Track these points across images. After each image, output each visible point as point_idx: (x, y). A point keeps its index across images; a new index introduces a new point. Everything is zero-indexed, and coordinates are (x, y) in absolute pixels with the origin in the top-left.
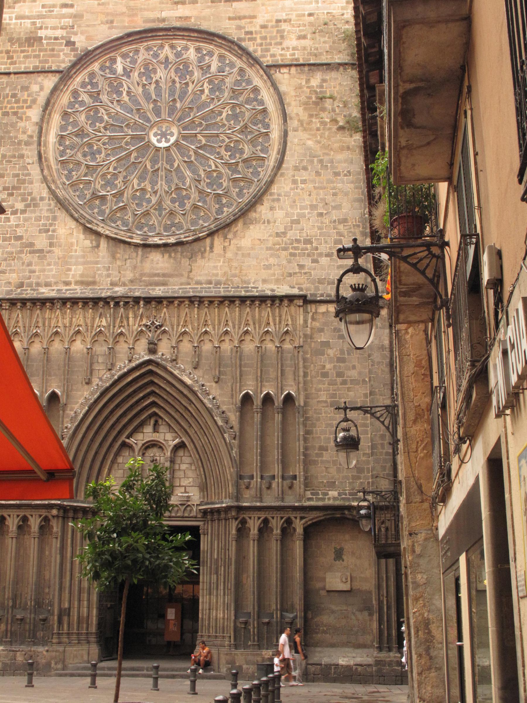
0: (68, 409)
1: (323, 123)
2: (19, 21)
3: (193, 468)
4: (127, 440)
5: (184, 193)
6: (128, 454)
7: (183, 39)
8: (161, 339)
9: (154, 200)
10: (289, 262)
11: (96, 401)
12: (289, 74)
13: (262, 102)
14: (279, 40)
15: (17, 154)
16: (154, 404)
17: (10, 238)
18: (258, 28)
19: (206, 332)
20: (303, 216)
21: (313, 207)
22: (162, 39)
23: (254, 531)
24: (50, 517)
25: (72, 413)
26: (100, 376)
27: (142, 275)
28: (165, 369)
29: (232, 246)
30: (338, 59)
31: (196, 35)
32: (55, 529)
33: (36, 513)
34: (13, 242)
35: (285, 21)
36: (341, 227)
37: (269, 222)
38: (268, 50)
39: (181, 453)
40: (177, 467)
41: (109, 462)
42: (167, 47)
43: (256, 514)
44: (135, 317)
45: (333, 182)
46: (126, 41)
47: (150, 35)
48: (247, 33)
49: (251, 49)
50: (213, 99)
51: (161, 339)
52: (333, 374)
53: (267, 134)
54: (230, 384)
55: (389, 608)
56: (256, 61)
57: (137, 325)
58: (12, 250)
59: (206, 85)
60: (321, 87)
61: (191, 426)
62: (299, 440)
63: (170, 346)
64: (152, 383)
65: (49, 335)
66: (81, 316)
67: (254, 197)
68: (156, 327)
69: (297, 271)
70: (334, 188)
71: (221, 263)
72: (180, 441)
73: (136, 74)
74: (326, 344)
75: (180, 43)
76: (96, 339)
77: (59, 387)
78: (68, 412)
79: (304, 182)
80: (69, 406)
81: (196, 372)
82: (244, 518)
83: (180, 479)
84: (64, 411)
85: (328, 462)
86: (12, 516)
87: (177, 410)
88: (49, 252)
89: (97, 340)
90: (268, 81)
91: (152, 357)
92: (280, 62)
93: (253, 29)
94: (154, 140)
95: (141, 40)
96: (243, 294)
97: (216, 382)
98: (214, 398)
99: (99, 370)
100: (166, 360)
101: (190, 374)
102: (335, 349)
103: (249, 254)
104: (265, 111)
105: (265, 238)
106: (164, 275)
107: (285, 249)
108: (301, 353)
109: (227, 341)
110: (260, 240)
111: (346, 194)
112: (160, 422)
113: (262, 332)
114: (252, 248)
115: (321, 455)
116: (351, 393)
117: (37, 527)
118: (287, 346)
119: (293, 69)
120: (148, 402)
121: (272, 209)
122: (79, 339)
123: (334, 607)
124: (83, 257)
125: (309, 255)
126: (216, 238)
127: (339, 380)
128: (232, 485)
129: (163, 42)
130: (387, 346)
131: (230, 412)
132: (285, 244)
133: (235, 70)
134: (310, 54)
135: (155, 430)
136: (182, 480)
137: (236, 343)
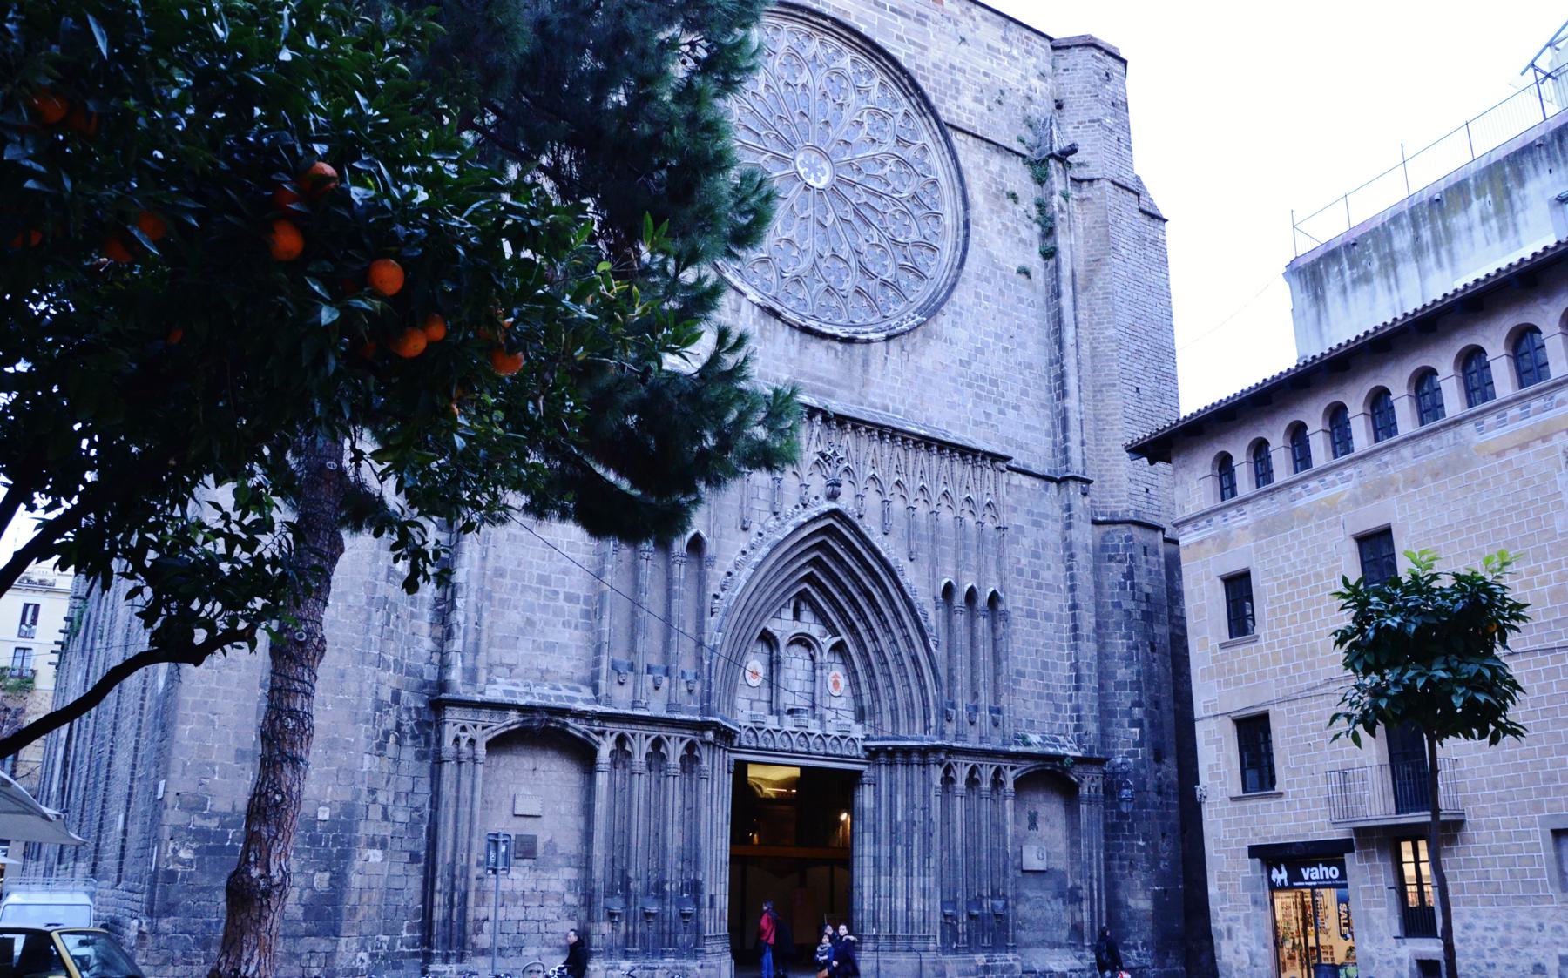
0: (717, 566)
1: (1004, 225)
4: (770, 628)
5: (842, 265)
9: (805, 264)
10: (975, 405)
12: (966, 142)
13: (929, 168)
14: (954, 92)
16: (810, 578)
18: (930, 66)
19: (898, 483)
21: (998, 337)
23: (961, 784)
24: (698, 743)
25: (723, 573)
27: (801, 374)
28: (853, 527)
29: (911, 364)
30: (1018, 147)
31: (857, 41)
32: (705, 764)
33: (676, 735)
35: (960, 70)
36: (1026, 372)
38: (943, 101)
42: (816, 42)
43: (962, 760)
45: (1017, 310)
48: (919, 67)
49: (927, 90)
50: (874, 141)
52: (1028, 570)
53: (936, 216)
54: (926, 566)
55: (1099, 894)
56: (933, 111)
59: (864, 118)
60: (1001, 177)
61: (864, 619)
62: (1007, 659)
63: (853, 495)
67: (933, 298)
69: (984, 420)
70: (1018, 318)
71: (899, 385)
72: (838, 639)
73: (777, 62)
74: (1020, 529)
78: (716, 570)
79: (987, 298)
81: (886, 538)
82: (949, 765)
85: (1026, 693)
86: (638, 736)
87: (844, 591)
90: (943, 143)
91: (833, 506)
92: (956, 124)
93: (923, 64)
94: (802, 171)
96: (942, 438)
97: (911, 560)
100: (853, 513)
103: (931, 381)
104: (934, 182)
106: (829, 382)
107: (970, 386)
108: (1006, 538)
109: (921, 500)
111: (1031, 331)
112: (803, 606)
113: (963, 498)
114: (934, 374)
115: (1017, 682)
116: (1047, 602)
117: (678, 758)
118: (990, 525)
119: (970, 139)
121: (954, 324)
123: (1030, 894)
125: (995, 402)
126: (892, 343)
127: (1035, 582)
128: (936, 716)
129: (813, 32)
130: (1090, 548)
133: (901, 111)
134: (988, 127)
135: (797, 616)
137: (934, 507)
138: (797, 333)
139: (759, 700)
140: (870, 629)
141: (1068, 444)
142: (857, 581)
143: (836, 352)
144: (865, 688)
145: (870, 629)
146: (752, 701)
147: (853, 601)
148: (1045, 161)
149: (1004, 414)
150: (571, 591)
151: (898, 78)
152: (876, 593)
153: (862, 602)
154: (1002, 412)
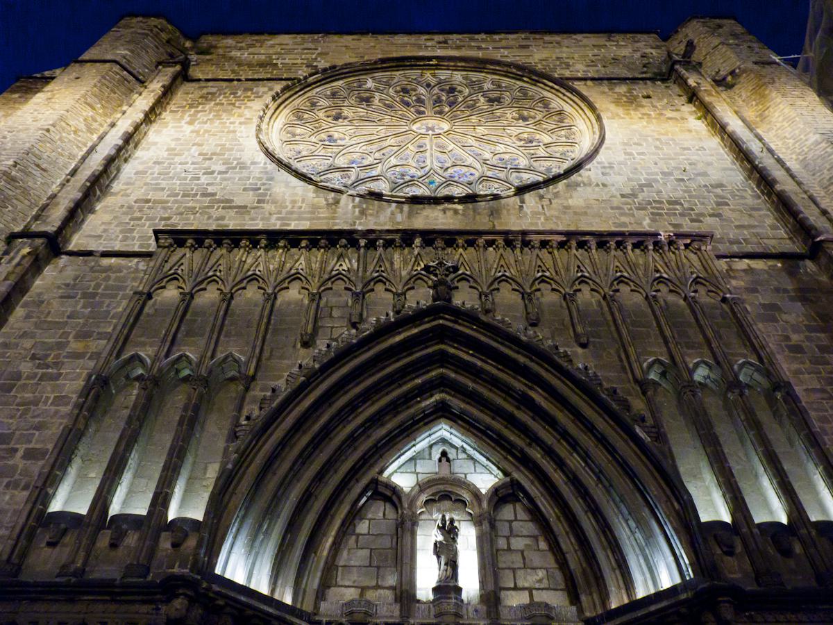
2: (252, 56)
3: (543, 545)
6: (381, 514)
7: (448, 69)
8: (457, 288)
10: (653, 220)
11: (328, 367)
12: (585, 84)
14: (564, 66)
15: (226, 130)
17: (196, 195)
18: (537, 61)
20: (657, 181)
22: (422, 69)
26: (334, 336)
29: (554, 205)
31: (463, 64)
34: (198, 197)
36: (719, 191)
37: (604, 185)
39: (507, 512)
40: (502, 543)
41: (337, 523)
44: (405, 262)
46: (379, 66)
47: (408, 64)
51: (457, 288)
54: (612, 351)
57: (410, 267)
58: (194, 205)
61: (536, 440)
64: (443, 359)
65: (238, 279)
66: (302, 258)
68: (447, 269)
75: (443, 74)
76: (329, 285)
77: (241, 352)
80: (259, 384)
83: (514, 570)
84: (247, 389)
88: (257, 207)
89: (331, 289)
95: (398, 68)
97: (584, 346)
98: (586, 368)
99: (332, 328)
101: (526, 329)
102: (794, 315)
105: (604, 198)
110: (598, 200)
112: (452, 454)
119: (589, 83)
120: (432, 400)
122: (296, 286)
124: (313, 213)
125: (682, 215)
126: (527, 196)
131: (631, 395)
132: (639, 204)
136: (520, 573)
138: (406, 207)
139: (378, 587)
140: (549, 452)
141: (778, 187)
142: (506, 390)
143: (456, 212)
144: (568, 543)
145: (549, 452)
146: (363, 589)
147: (512, 421)
148: (672, 69)
149: (701, 222)
150: (38, 446)
151: (507, 72)
152: (538, 397)
153: (523, 416)
154: (692, 221)
